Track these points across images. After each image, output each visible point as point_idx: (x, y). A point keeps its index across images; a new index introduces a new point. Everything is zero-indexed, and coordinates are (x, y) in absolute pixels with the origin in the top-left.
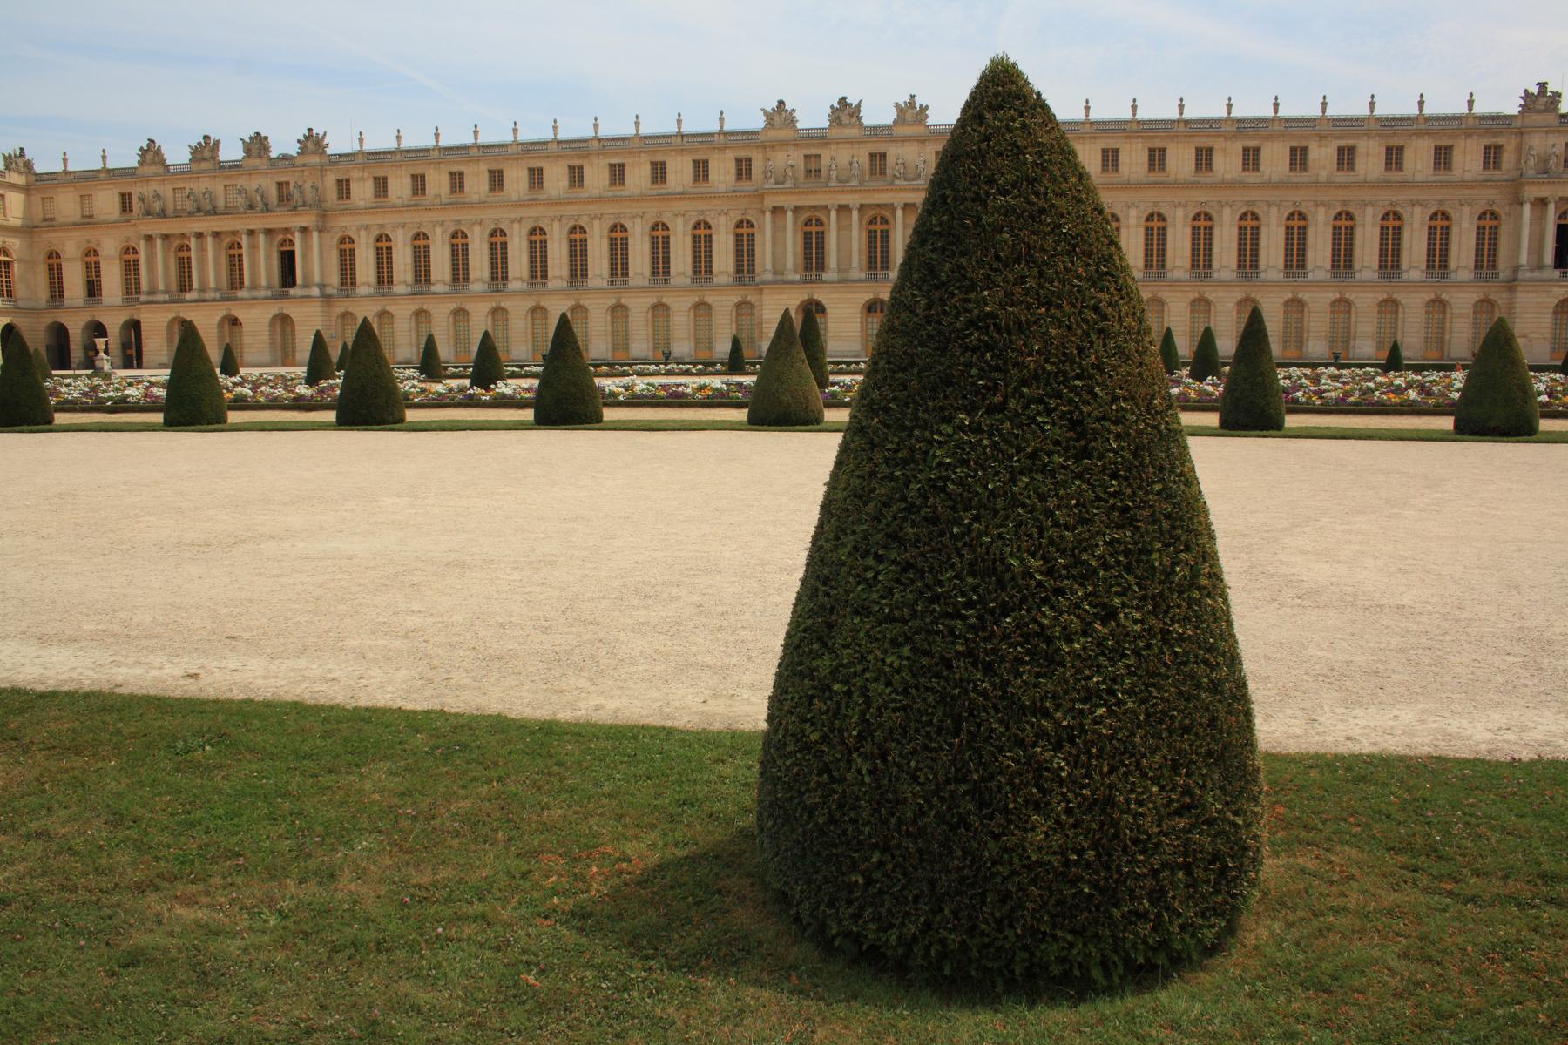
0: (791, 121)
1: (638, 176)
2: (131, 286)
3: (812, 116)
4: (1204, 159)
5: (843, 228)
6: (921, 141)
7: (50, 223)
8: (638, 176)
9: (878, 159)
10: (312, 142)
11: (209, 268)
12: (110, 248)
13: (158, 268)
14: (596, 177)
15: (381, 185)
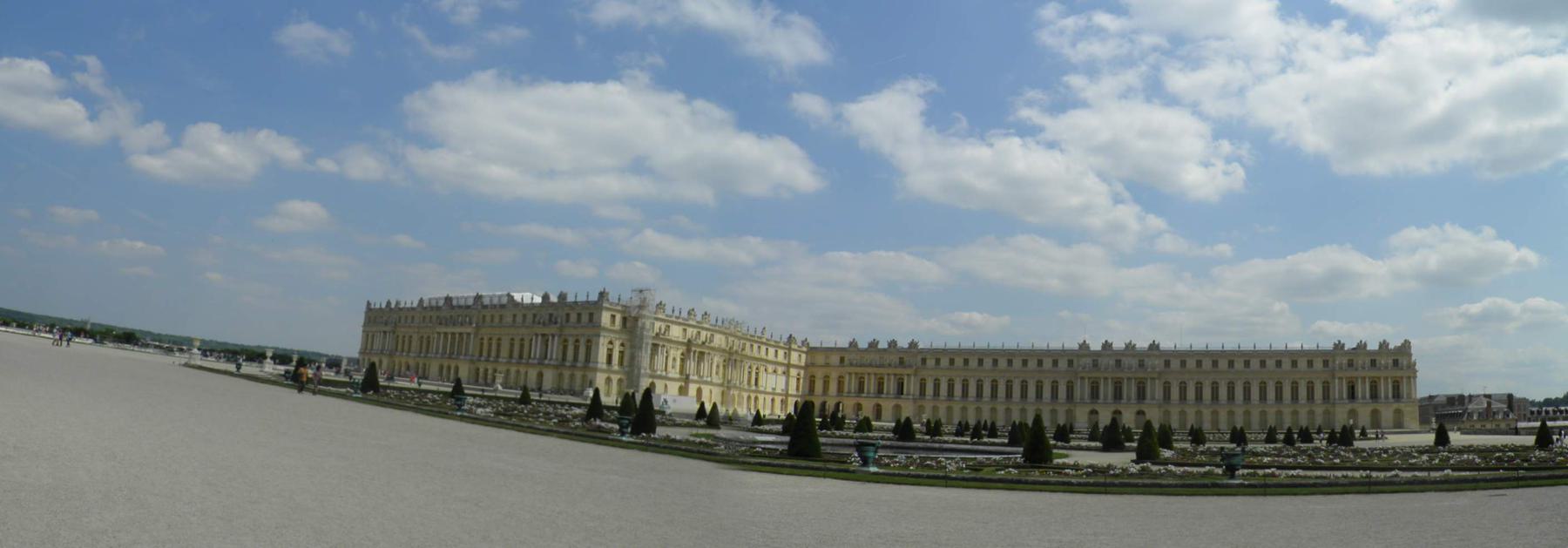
0: (1088, 347)
1: (1032, 364)
2: (840, 390)
3: (1096, 346)
4: (1231, 364)
5: (1106, 385)
6: (1134, 356)
7: (813, 365)
8: (1032, 364)
9: (1118, 362)
10: (913, 345)
11: (870, 385)
12: (834, 375)
13: (851, 384)
14: (1017, 363)
15: (938, 361)
